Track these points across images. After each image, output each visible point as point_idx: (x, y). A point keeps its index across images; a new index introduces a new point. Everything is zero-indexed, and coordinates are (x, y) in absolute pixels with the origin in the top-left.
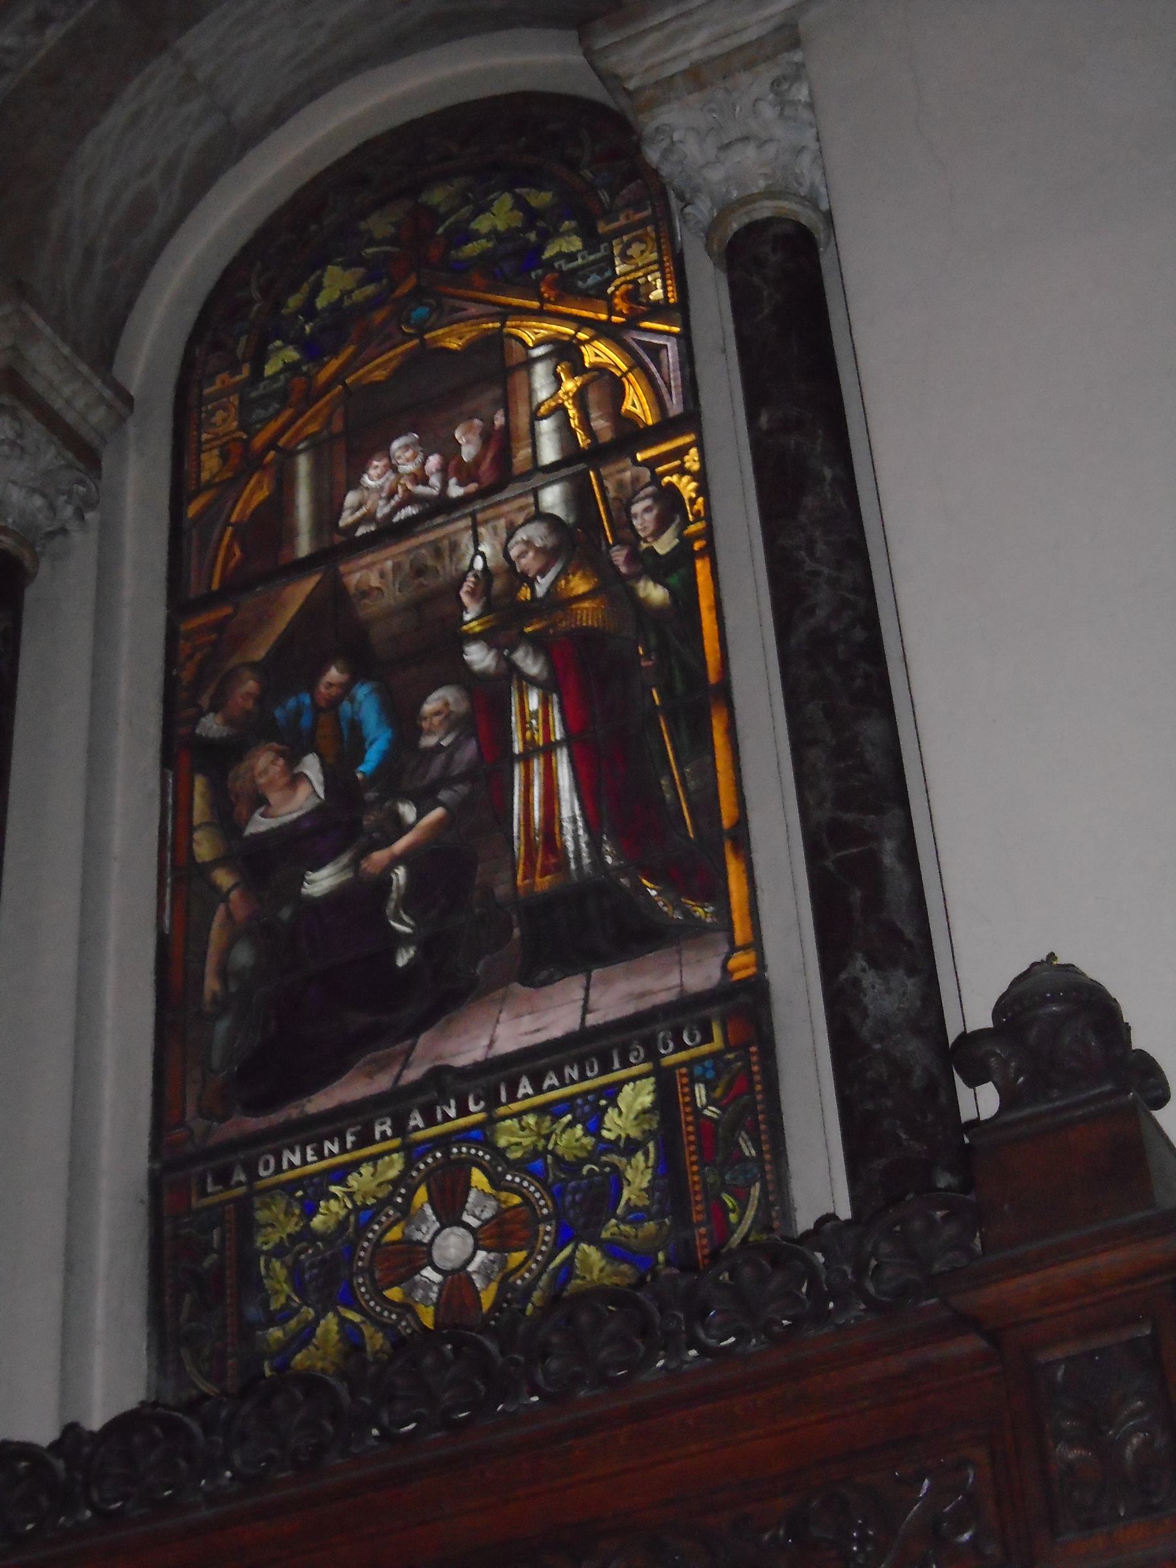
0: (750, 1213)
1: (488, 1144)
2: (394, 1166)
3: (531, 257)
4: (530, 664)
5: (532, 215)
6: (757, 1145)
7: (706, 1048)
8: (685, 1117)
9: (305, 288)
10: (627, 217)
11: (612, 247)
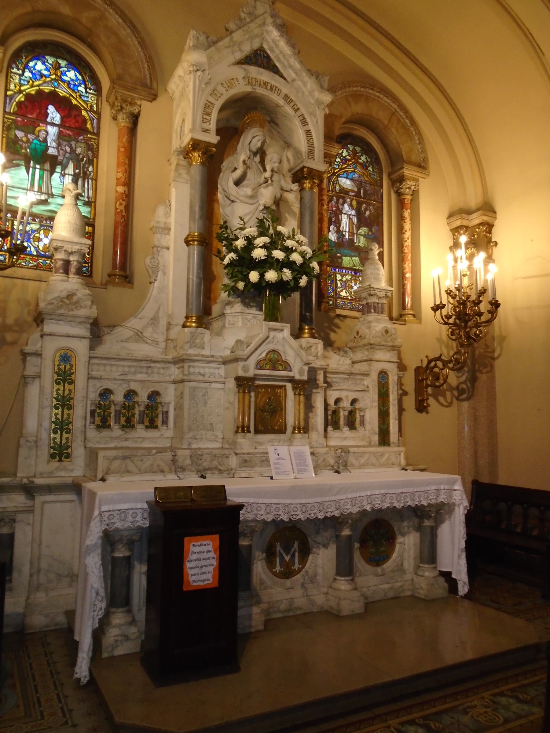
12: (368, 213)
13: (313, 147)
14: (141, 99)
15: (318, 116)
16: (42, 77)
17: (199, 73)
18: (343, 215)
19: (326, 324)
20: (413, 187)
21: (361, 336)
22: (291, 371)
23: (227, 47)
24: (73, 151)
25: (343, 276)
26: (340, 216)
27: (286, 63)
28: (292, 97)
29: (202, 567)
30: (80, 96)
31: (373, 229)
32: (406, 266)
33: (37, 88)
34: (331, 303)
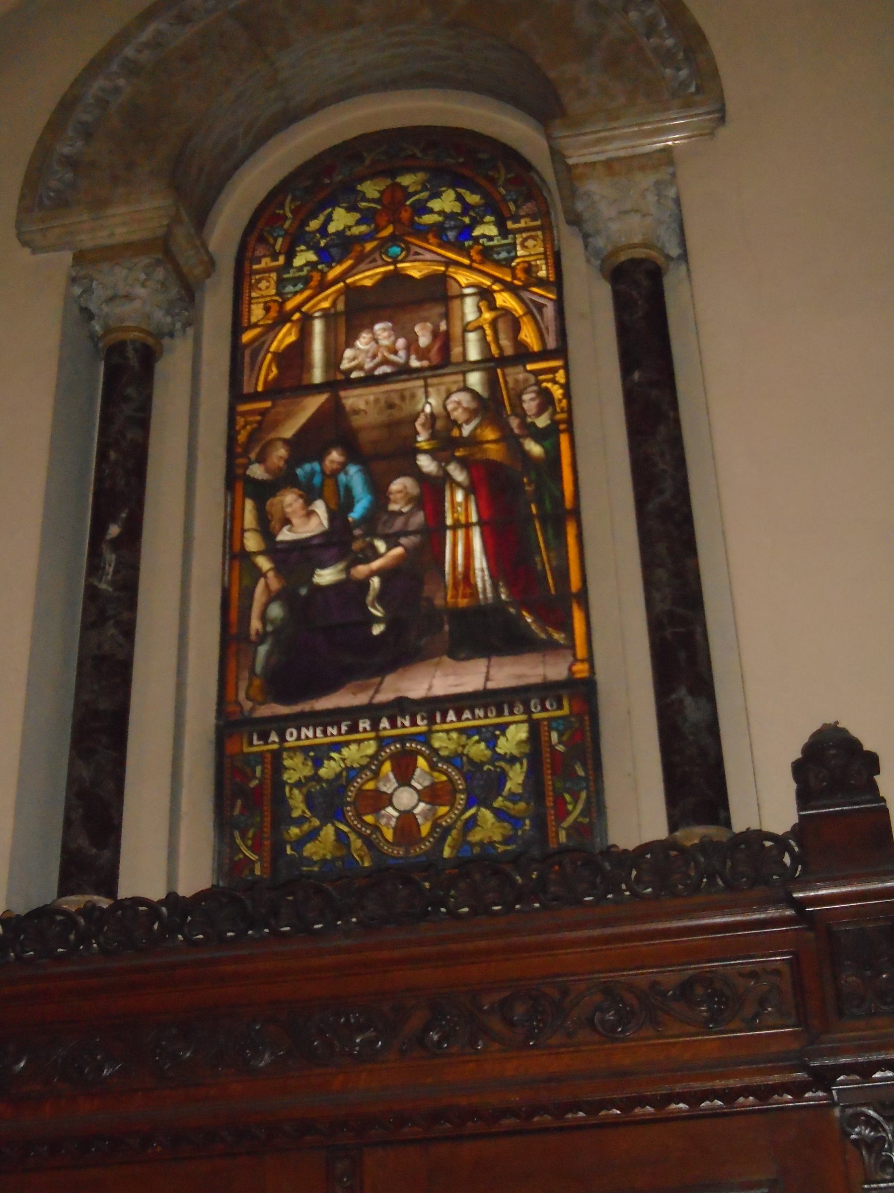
0: (580, 807)
1: (427, 743)
2: (370, 748)
3: (465, 232)
4: (459, 475)
5: (467, 208)
6: (585, 770)
7: (559, 713)
8: (546, 750)
9: (322, 218)
10: (526, 223)
11: (515, 238)
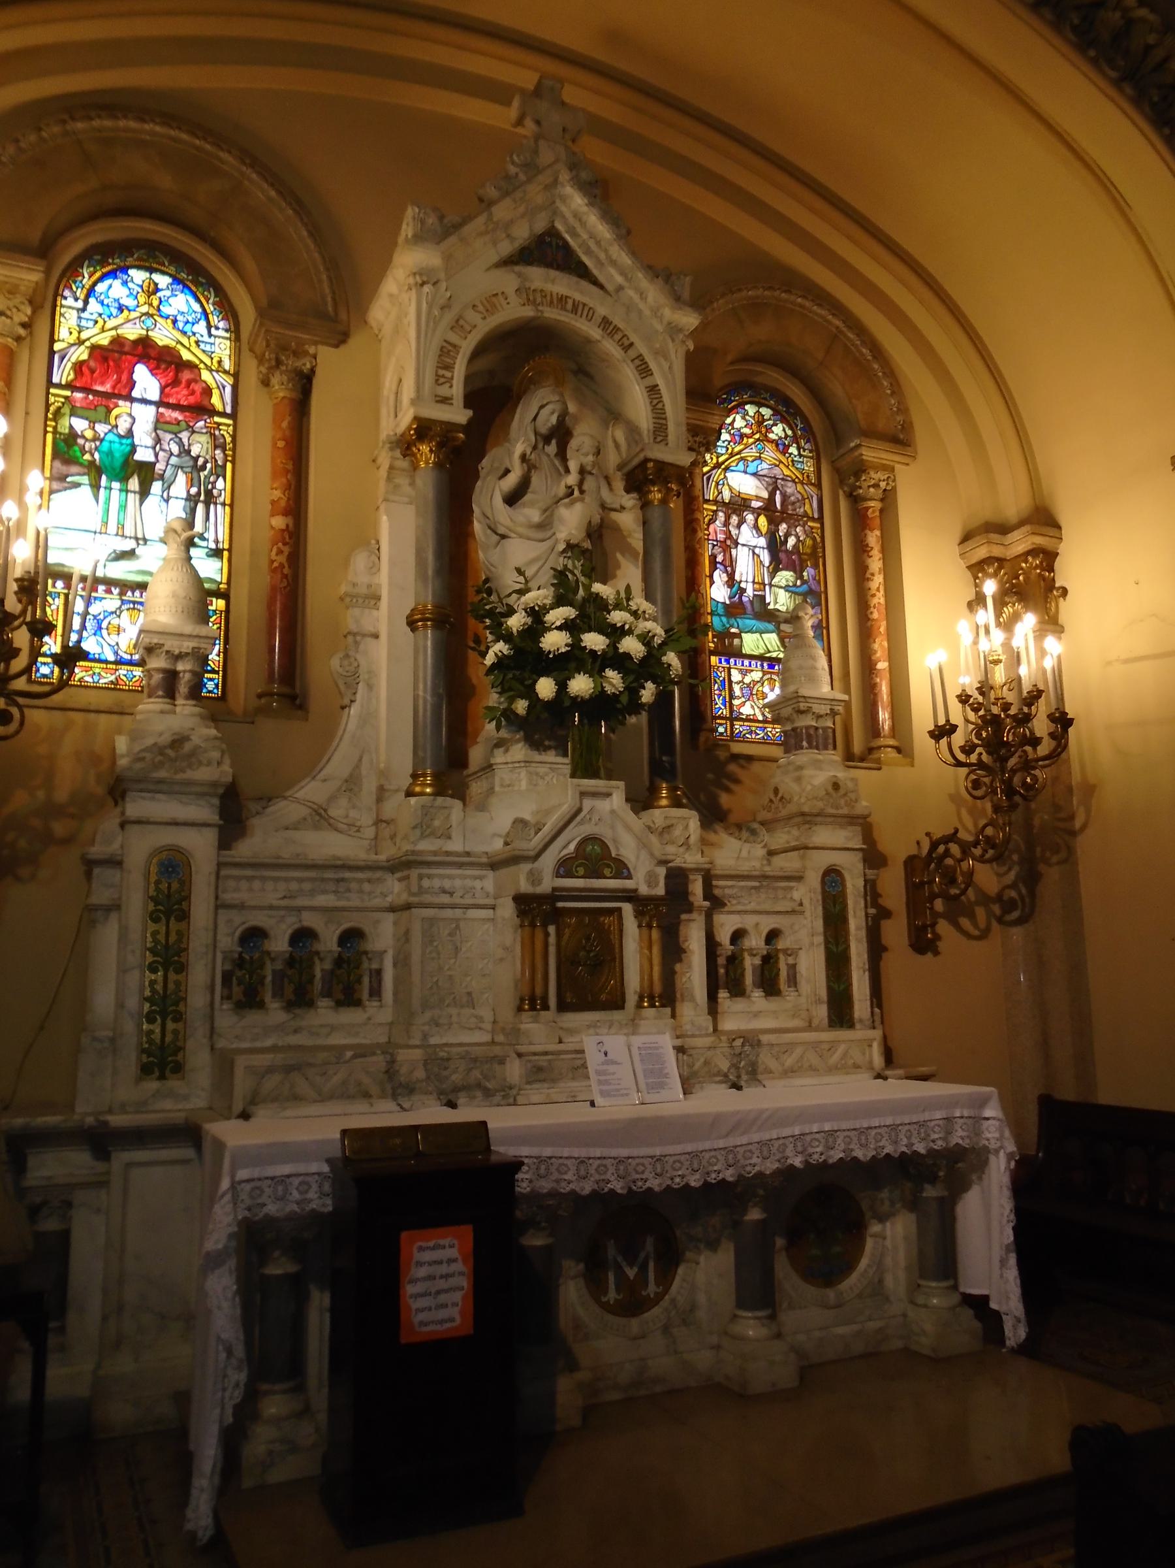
5: (786, 436)
12: (792, 541)
13: (665, 419)
14: (316, 343)
15: (673, 356)
16: (122, 311)
17: (426, 289)
18: (739, 546)
19: (710, 776)
20: (883, 485)
21: (782, 798)
22: (629, 877)
23: (481, 234)
24: (185, 452)
25: (744, 673)
26: (734, 552)
27: (602, 256)
28: (617, 321)
29: (438, 1292)
30: (197, 343)
31: (805, 574)
32: (876, 646)
33: (113, 333)
34: (721, 730)
